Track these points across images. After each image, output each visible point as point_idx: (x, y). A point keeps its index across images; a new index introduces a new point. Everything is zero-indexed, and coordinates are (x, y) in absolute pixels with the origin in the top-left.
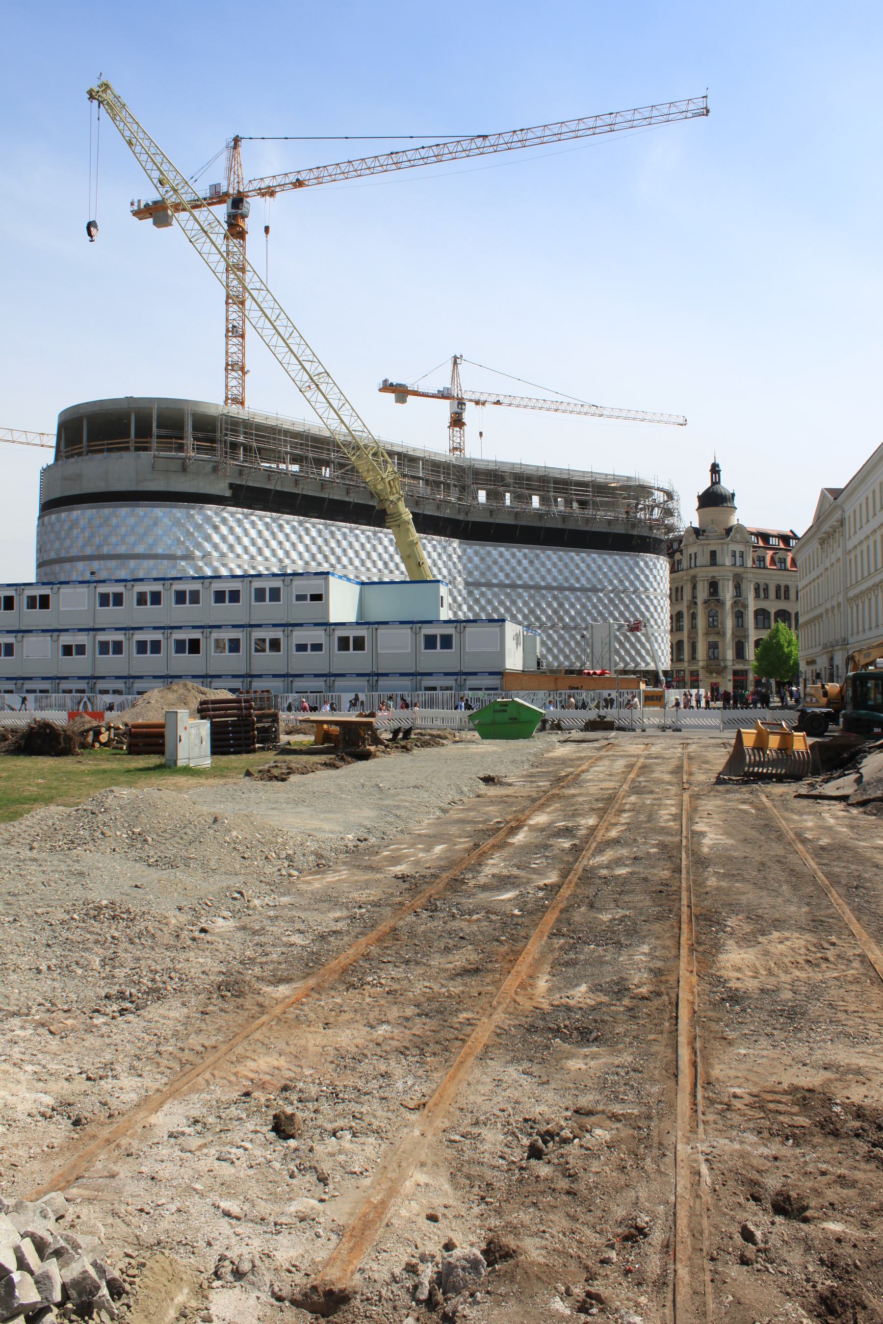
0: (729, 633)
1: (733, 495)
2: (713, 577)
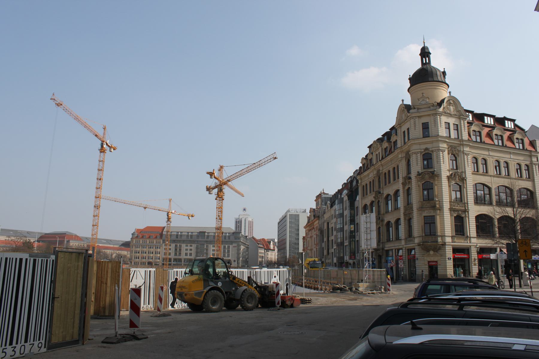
0: (446, 206)
1: (444, 73)
2: (426, 149)
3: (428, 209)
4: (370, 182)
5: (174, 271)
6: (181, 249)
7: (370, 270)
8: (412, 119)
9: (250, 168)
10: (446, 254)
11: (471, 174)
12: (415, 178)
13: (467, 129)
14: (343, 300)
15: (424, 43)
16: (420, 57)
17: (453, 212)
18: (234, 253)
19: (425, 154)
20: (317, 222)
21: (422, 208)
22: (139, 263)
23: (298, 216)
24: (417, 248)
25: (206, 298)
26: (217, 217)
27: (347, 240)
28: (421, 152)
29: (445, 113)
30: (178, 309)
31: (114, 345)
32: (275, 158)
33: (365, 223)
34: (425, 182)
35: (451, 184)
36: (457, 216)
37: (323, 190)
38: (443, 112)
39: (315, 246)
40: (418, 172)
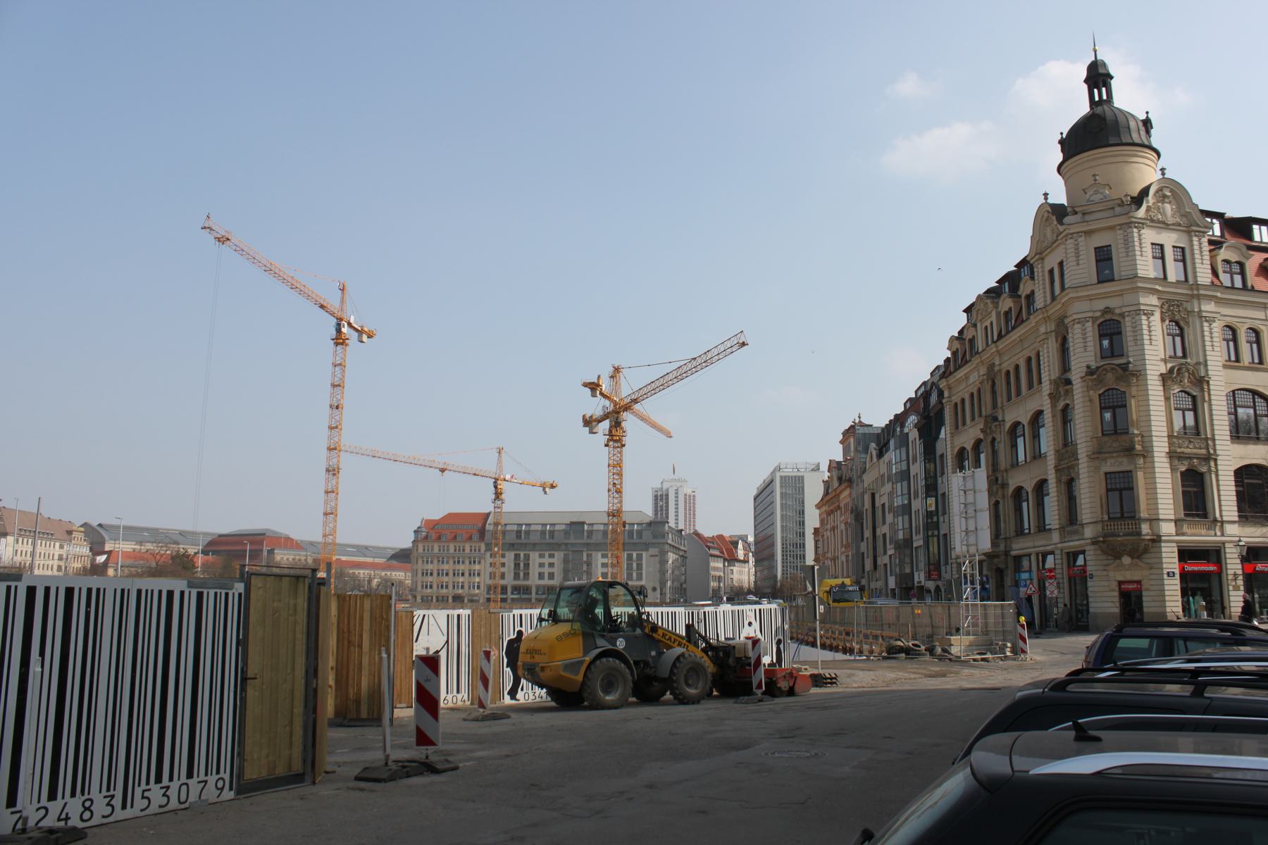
0: (1160, 447)
1: (1147, 123)
2: (1107, 310)
3: (1115, 455)
4: (972, 395)
5: (514, 615)
6: (528, 564)
7: (977, 605)
8: (1071, 238)
9: (685, 369)
10: (1162, 563)
11: (1221, 369)
12: (1080, 380)
13: (1208, 258)
14: (913, 676)
15: (1095, 51)
16: (1085, 87)
17: (1179, 461)
18: (651, 569)
19: (1104, 323)
20: (847, 493)
21: (1100, 453)
22: (432, 597)
23: (801, 479)
24: (1090, 550)
25: (590, 676)
26: (611, 486)
27: (919, 533)
28: (1094, 319)
29: (1152, 221)
30: (525, 702)
31: (382, 785)
32: (743, 344)
33: (962, 493)
34: (1105, 392)
35: (1172, 392)
36: (1187, 470)
37: (859, 417)
38: (1147, 219)
39: (843, 549)
40: (1088, 367)
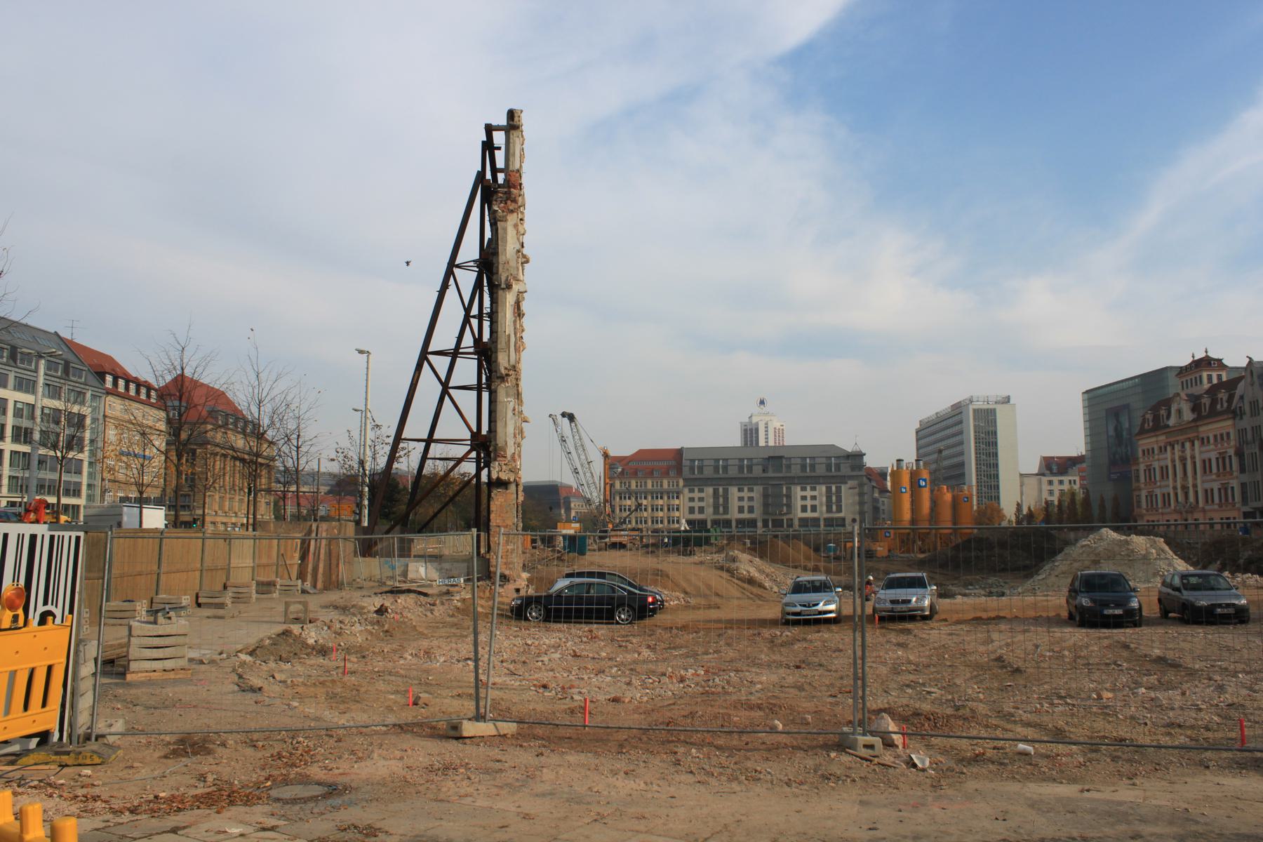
23: (993, 411)
